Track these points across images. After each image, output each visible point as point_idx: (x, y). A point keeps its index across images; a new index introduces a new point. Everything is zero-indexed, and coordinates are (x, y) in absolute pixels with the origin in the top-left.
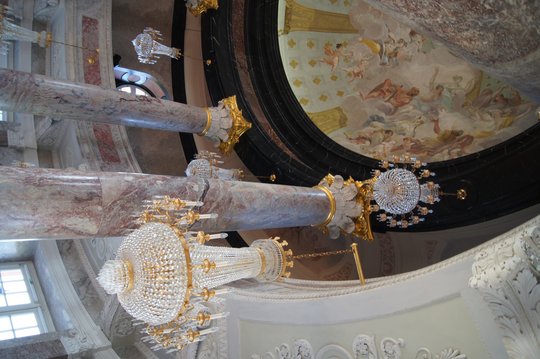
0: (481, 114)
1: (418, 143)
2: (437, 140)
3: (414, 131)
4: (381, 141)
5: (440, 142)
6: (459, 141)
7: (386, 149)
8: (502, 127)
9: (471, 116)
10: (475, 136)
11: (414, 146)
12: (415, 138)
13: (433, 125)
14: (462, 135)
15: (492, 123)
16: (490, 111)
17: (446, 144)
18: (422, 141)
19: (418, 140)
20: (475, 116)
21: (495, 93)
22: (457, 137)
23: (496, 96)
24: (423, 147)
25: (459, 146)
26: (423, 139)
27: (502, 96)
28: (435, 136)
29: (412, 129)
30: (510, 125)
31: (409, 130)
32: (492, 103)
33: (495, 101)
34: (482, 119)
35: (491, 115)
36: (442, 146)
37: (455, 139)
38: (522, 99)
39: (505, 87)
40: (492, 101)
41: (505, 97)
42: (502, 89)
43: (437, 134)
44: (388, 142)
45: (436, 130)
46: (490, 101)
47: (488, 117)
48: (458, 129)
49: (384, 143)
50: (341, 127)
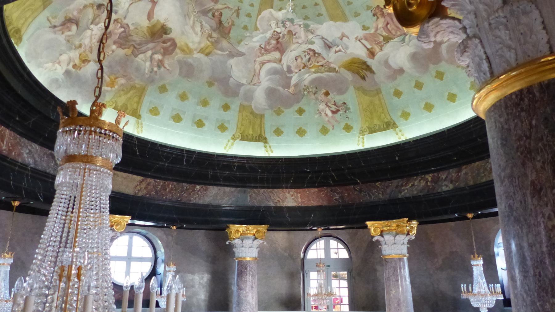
0: (196, 19)
1: (127, 30)
2: (145, 30)
3: (128, 9)
4: (90, 21)
5: (148, 35)
6: (164, 42)
7: (93, 37)
8: (201, 51)
9: (186, 16)
10: (178, 45)
11: (123, 34)
12: (125, 21)
13: (150, 6)
14: (169, 36)
15: (197, 39)
16: (204, 23)
17: (152, 42)
18: (132, 28)
19: (128, 25)
20: (190, 19)
21: (219, 6)
22: (164, 36)
23: (218, 10)
24: (130, 38)
25: (162, 50)
26: (133, 24)
27: (221, 14)
28: (145, 23)
29: (127, 5)
30: (207, 55)
31: (123, 5)
32: (210, 15)
33: (213, 15)
34: (193, 27)
35: (201, 28)
36: (147, 42)
37: (162, 37)
38: (230, 35)
39: (228, 7)
40: (211, 13)
41: (223, 19)
42: (226, 8)
43: (148, 22)
44: (96, 25)
45: (150, 16)
46: (210, 10)
47: (198, 29)
48: (169, 25)
49: (92, 26)
50: (44, 9)
